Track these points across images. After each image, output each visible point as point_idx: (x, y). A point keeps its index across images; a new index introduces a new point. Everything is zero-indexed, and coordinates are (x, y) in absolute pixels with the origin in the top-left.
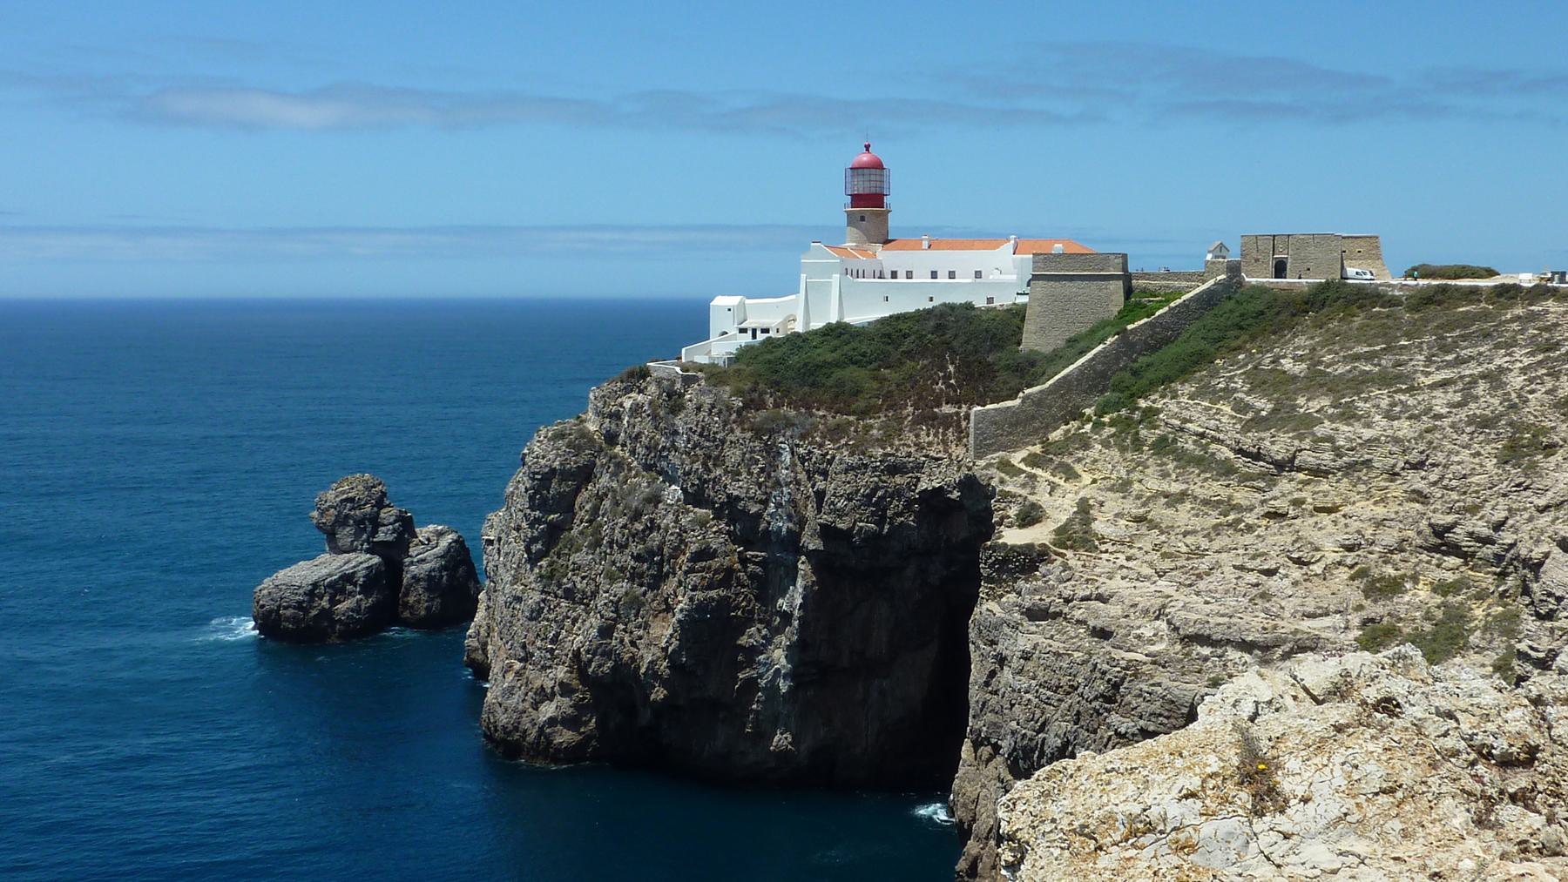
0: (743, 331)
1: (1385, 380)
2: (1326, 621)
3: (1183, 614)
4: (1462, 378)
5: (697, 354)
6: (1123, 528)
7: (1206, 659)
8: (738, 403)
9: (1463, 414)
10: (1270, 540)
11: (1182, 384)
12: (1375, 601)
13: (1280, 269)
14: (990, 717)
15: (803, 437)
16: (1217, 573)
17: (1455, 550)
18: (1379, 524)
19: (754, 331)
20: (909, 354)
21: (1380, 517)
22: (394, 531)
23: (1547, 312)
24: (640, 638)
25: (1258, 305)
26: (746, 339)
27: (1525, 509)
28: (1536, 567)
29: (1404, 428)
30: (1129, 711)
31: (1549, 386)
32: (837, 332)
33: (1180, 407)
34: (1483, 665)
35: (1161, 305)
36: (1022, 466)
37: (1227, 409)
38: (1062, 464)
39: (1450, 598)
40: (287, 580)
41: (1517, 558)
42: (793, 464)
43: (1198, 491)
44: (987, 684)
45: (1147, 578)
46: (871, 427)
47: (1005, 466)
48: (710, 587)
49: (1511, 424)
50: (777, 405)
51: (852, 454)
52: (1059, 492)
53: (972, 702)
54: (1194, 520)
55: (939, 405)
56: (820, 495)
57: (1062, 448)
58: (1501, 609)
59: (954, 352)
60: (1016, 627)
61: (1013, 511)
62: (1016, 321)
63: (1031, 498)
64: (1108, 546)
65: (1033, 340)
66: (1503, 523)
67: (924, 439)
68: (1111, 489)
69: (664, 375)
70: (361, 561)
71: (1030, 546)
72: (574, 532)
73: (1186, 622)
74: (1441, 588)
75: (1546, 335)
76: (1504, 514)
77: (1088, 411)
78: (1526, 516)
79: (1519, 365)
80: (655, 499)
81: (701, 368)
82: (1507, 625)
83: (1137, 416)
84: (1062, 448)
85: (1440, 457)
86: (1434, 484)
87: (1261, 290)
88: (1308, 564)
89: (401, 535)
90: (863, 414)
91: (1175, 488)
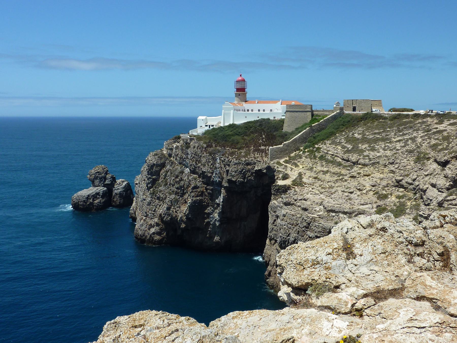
0: (206, 126)
1: (383, 140)
2: (367, 206)
3: (327, 204)
4: (404, 139)
5: (194, 132)
6: (311, 180)
7: (334, 216)
9: (405, 149)
10: (351, 184)
12: (380, 201)
13: (354, 109)
14: (274, 232)
15: (223, 155)
16: (337, 193)
17: (402, 186)
18: (381, 179)
19: (209, 126)
20: (252, 132)
22: (110, 181)
23: (428, 121)
24: (178, 210)
26: (207, 128)
28: (425, 191)
29: (388, 153)
30: (312, 231)
31: (428, 141)
32: (232, 126)
33: (327, 147)
34: (410, 218)
36: (283, 163)
37: (340, 148)
39: (401, 200)
40: (81, 194)
41: (419, 189)
43: (331, 170)
44: (273, 223)
45: (318, 194)
46: (242, 152)
47: (279, 163)
48: (197, 196)
49: (418, 152)
50: (216, 146)
51: (236, 160)
52: (293, 170)
53: (269, 229)
54: (331, 178)
55: (260, 147)
56: (228, 171)
57: (294, 158)
58: (415, 203)
59: (264, 132)
60: (281, 207)
62: (282, 123)
63: (286, 172)
64: (307, 185)
65: (286, 129)
66: (415, 179)
67: (256, 156)
68: (308, 170)
70: (101, 189)
71: (285, 185)
73: (328, 206)
74: (398, 197)
76: (416, 177)
77: (301, 148)
78: (422, 177)
80: (182, 172)
81: (195, 136)
82: (417, 207)
83: (315, 149)
84: (294, 158)
85: (398, 161)
86: (397, 168)
87: (349, 115)
89: (112, 182)
90: (239, 149)
91: (325, 169)
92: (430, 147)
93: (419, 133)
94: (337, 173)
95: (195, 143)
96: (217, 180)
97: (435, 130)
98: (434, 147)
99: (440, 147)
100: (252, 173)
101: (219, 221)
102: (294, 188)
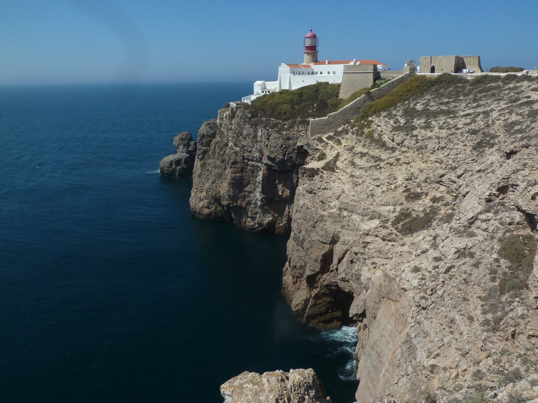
0: (263, 92)
1: (448, 113)
7: (344, 217)
8: (249, 115)
9: (467, 128)
13: (433, 70)
15: (264, 127)
18: (421, 171)
20: (305, 100)
21: (422, 168)
23: (522, 86)
25: (417, 84)
27: (471, 171)
31: (506, 118)
34: (431, 236)
35: (385, 82)
36: (325, 140)
37: (392, 122)
42: (262, 136)
45: (343, 183)
46: (285, 124)
47: (320, 140)
48: (236, 173)
51: (276, 133)
52: (333, 149)
55: (308, 118)
56: (267, 146)
57: (340, 133)
58: (451, 211)
63: (324, 151)
65: (342, 95)
66: (461, 176)
67: (300, 129)
68: (347, 150)
71: (313, 169)
75: (516, 96)
77: (352, 121)
78: (471, 173)
79: (500, 108)
80: (227, 145)
83: (366, 123)
88: (391, 184)
91: (366, 151)
92: (505, 126)
93: (501, 104)
94: (377, 157)
95: (240, 112)
96: (257, 155)
97: (526, 100)
98: (509, 127)
99: (517, 128)
100: (294, 150)
101: (262, 201)
102: (322, 172)
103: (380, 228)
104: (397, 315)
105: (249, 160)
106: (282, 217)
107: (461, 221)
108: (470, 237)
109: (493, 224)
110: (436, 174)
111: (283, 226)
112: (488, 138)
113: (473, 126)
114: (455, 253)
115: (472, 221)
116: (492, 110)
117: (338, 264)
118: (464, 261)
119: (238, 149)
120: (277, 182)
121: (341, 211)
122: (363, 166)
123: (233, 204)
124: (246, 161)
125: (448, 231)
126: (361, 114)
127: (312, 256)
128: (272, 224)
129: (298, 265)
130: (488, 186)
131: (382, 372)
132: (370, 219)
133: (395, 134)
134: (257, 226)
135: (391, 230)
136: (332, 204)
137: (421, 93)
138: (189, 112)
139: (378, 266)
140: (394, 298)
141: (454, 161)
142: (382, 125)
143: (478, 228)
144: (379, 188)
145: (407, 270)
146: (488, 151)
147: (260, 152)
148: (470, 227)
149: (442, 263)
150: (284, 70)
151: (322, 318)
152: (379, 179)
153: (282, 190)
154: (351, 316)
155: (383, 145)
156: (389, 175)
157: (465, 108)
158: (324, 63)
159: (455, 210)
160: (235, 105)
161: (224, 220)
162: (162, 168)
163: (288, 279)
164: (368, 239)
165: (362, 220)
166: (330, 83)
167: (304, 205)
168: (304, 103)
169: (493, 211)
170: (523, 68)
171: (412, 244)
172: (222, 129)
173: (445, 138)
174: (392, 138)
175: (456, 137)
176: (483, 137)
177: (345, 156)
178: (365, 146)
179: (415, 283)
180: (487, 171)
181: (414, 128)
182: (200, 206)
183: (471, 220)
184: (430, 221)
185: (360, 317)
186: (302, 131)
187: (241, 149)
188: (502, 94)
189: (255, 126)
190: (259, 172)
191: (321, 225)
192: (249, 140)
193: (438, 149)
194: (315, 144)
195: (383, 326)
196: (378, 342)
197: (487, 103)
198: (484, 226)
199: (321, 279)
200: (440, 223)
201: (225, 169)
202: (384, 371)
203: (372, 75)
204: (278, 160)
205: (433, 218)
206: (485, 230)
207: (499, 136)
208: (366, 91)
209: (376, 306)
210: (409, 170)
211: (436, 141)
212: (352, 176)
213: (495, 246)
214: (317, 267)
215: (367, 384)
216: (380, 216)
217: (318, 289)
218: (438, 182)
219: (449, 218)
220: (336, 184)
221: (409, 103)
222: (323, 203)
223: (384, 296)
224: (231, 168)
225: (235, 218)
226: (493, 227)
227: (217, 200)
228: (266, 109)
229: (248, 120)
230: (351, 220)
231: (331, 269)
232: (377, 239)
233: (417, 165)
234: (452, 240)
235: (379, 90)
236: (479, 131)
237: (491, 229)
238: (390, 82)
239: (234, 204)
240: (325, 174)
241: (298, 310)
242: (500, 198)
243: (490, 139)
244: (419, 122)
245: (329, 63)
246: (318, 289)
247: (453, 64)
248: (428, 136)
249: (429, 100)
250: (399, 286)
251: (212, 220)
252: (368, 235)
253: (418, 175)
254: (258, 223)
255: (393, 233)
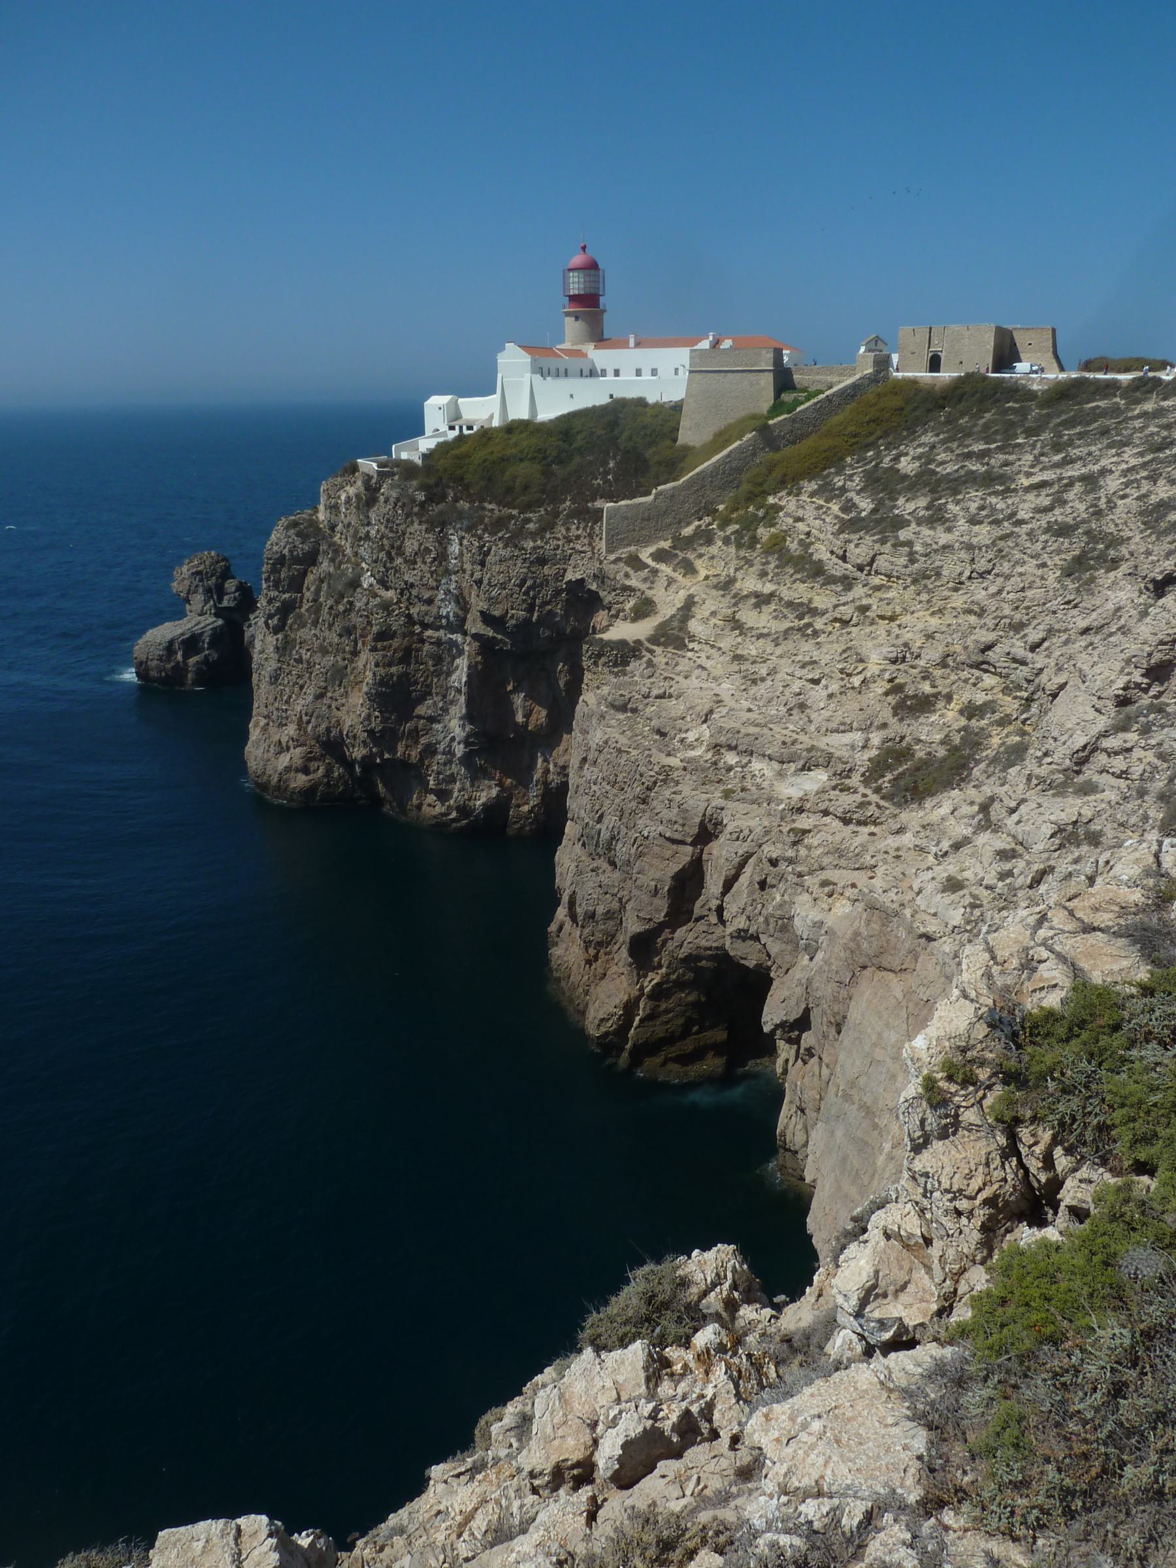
0: (452, 428)
1: (988, 480)
2: (848, 738)
7: (730, 769)
8: (421, 496)
11: (809, 481)
13: (935, 364)
15: (468, 530)
18: (930, 636)
19: (461, 428)
21: (932, 629)
22: (235, 598)
24: (343, 705)
25: (897, 402)
27: (1065, 631)
31: (1143, 491)
34: (972, 803)
36: (649, 561)
37: (835, 507)
38: (685, 560)
39: (974, 723)
42: (461, 554)
46: (529, 520)
47: (635, 562)
48: (390, 665)
51: (505, 547)
52: (674, 587)
55: (594, 500)
56: (479, 582)
57: (687, 543)
58: (1018, 738)
61: (630, 604)
63: (649, 593)
65: (686, 436)
67: (574, 532)
68: (716, 587)
69: (366, 471)
71: (623, 643)
72: (303, 610)
73: (721, 730)
75: (1165, 433)
76: (1041, 635)
77: (721, 507)
78: (1064, 637)
79: (1124, 466)
80: (355, 584)
81: (399, 463)
83: (761, 513)
85: (1006, 567)
88: (849, 675)
90: (528, 507)
91: (768, 588)
92: (1141, 513)
93: (1126, 456)
94: (801, 604)
95: (392, 487)
96: (449, 609)
100: (558, 592)
101: (467, 743)
102: (651, 652)
103: (832, 793)
104: (911, 1005)
105: (425, 626)
106: (527, 787)
107: (1056, 758)
108: (1085, 794)
109: (1140, 759)
110: (969, 642)
111: (530, 812)
112: (1101, 546)
113: (1058, 515)
114: (1052, 836)
115: (1083, 757)
116: (1104, 472)
117: (724, 894)
118: (1076, 854)
119: (390, 594)
120: (510, 688)
121: (718, 753)
122: (766, 631)
123: (381, 755)
124: (417, 629)
125: (1021, 786)
126: (746, 487)
127: (643, 880)
128: (498, 809)
129: (601, 910)
130: (1118, 666)
131: (881, 1149)
132: (803, 769)
133: (850, 541)
134: (454, 815)
135: (865, 795)
136: (691, 736)
137: (908, 429)
138: (233, 489)
139: (839, 889)
140: (896, 965)
141: (1017, 608)
142: (807, 516)
143: (1102, 772)
144: (817, 687)
145: (930, 888)
146: (1105, 578)
147: (457, 602)
148: (1078, 772)
149: (1020, 864)
150: (513, 362)
151: (674, 1050)
152: (815, 662)
153: (526, 711)
154: (767, 1029)
155: (816, 571)
156: (844, 651)
157: (1032, 466)
158: (624, 345)
159: (1029, 734)
160: (375, 465)
161: (356, 801)
162: (141, 663)
163: (567, 950)
164: (804, 822)
165: (781, 775)
166: (651, 400)
167: (606, 742)
168: (577, 459)
169: (1136, 727)
170: (1169, 360)
171: (924, 827)
172: (336, 539)
173: (987, 546)
174: (841, 553)
175: (1017, 545)
176: (1087, 543)
177: (710, 606)
178: (766, 574)
179: (956, 917)
180: (1106, 630)
181: (900, 523)
182: (280, 768)
183: (1081, 754)
184: (964, 766)
185: (791, 1030)
186: (578, 537)
187: (402, 594)
188: (1126, 428)
189: (439, 525)
190: (458, 661)
191: (667, 793)
192: (426, 568)
193: (970, 578)
194: (620, 573)
195: (874, 1037)
196: (862, 1081)
197: (1090, 454)
198: (1119, 763)
199: (670, 943)
200: (991, 769)
201: (355, 653)
202: (887, 1146)
203: (771, 375)
204: (514, 622)
205: (971, 757)
206: (1123, 775)
207: (1129, 538)
208: (758, 423)
209: (844, 993)
210: (897, 636)
211: (963, 555)
212: (738, 658)
213: (1152, 813)
214: (660, 909)
215: (839, 1188)
216: (828, 760)
217: (664, 970)
218: (977, 666)
219: (1016, 754)
220: (694, 682)
221: (878, 454)
222: (663, 734)
223: (866, 961)
224: (374, 649)
225: (389, 797)
226: (1142, 767)
227: (333, 746)
228: (468, 478)
229: (416, 509)
230: (749, 777)
231: (697, 911)
232: (828, 819)
233: (917, 623)
234: (1040, 805)
235: (793, 420)
236: (1076, 527)
237: (1136, 771)
238: (822, 396)
239: (387, 756)
240: (661, 656)
241: (606, 1034)
242: (1151, 693)
243: (1107, 548)
244: (911, 507)
245: (638, 345)
246: (664, 970)
247: (990, 347)
248: (942, 542)
249: (933, 447)
250: (910, 929)
251: (314, 806)
252: (800, 810)
253: (921, 648)
254: (458, 809)
255: (869, 803)
